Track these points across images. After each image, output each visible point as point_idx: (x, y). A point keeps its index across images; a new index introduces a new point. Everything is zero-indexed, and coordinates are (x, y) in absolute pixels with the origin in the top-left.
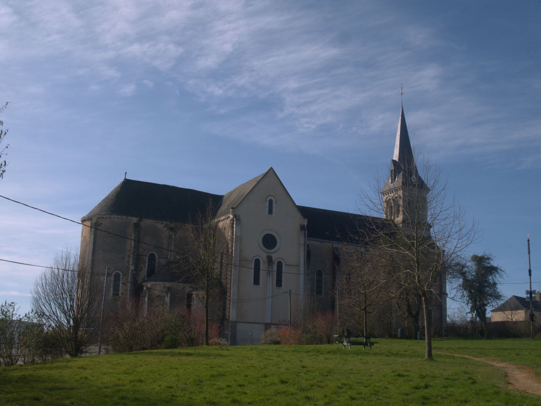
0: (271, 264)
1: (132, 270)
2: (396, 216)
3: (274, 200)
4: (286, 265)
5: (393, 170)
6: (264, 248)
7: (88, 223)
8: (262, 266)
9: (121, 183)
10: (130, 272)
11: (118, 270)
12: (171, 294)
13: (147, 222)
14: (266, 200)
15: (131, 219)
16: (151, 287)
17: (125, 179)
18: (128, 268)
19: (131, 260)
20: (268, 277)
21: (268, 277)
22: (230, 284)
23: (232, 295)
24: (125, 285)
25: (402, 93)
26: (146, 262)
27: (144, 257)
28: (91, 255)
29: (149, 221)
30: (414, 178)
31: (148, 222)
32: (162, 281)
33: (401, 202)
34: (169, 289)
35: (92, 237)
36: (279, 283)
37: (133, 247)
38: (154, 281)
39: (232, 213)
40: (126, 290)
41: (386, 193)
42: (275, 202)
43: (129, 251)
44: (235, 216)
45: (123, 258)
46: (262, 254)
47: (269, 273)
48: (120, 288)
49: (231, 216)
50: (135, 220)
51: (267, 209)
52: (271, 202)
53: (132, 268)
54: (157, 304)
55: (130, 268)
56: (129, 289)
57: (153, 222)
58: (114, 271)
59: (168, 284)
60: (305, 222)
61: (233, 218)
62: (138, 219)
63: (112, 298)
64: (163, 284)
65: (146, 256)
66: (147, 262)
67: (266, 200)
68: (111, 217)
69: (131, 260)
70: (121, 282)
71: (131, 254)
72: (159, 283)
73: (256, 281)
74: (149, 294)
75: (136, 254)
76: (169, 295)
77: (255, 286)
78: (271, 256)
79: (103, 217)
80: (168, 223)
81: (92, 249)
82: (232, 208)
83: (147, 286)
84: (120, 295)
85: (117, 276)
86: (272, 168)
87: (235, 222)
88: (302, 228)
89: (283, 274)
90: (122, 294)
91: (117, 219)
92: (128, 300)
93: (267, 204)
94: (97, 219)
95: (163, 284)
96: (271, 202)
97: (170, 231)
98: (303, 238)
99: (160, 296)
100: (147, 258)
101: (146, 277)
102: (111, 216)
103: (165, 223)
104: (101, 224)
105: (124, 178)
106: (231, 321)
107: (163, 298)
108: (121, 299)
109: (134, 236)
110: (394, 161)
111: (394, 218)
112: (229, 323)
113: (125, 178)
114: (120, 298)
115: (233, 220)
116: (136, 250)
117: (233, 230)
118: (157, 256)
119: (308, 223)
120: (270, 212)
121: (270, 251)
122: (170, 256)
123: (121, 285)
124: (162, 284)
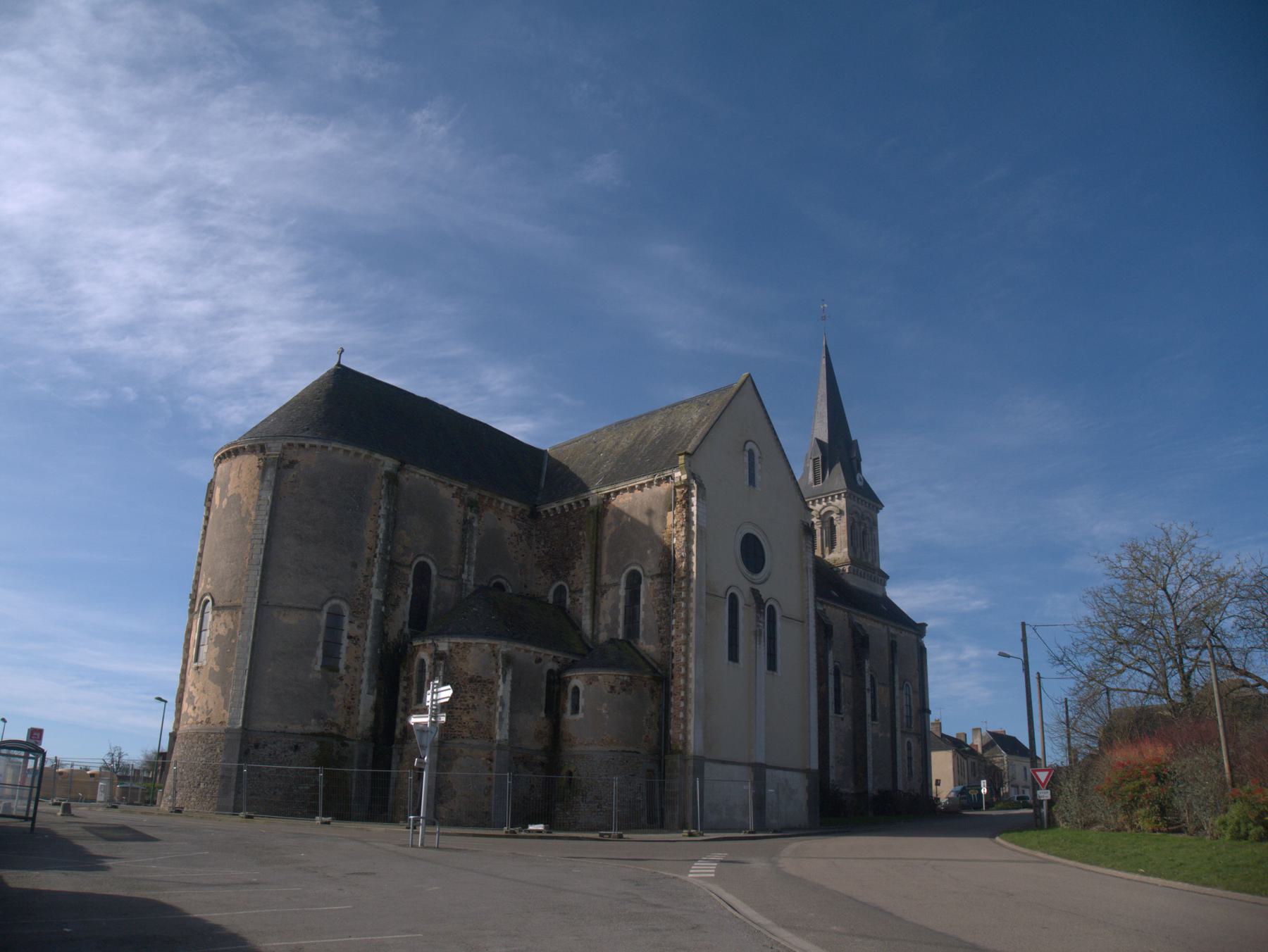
2: (827, 549)
5: (818, 458)
7: (250, 462)
9: (328, 372)
10: (372, 607)
11: (341, 598)
13: (417, 477)
14: (744, 450)
15: (379, 460)
16: (451, 651)
17: (339, 364)
18: (366, 596)
19: (376, 575)
22: (686, 655)
23: (692, 686)
24: (355, 644)
25: (825, 316)
26: (408, 586)
27: (404, 570)
28: (263, 547)
29: (422, 475)
31: (417, 476)
32: (488, 635)
33: (841, 526)
34: (508, 660)
35: (268, 496)
37: (381, 536)
38: (459, 633)
39: (685, 467)
41: (839, 495)
42: (760, 458)
43: (369, 548)
44: (692, 475)
45: (355, 565)
47: (757, 634)
48: (343, 649)
49: (680, 475)
50: (389, 464)
53: (376, 595)
54: (470, 702)
55: (371, 596)
56: (367, 654)
57: (430, 478)
58: (330, 599)
59: (503, 647)
61: (688, 480)
62: (397, 463)
63: (320, 677)
64: (490, 645)
65: (410, 566)
66: (411, 586)
67: (744, 450)
68: (327, 447)
69: (376, 575)
70: (345, 634)
71: (375, 556)
73: (733, 656)
74: (445, 673)
75: (388, 558)
76: (509, 677)
77: (731, 663)
78: (758, 591)
79: (303, 446)
80: (465, 487)
81: (265, 530)
82: (686, 454)
83: (436, 650)
84: (342, 671)
85: (335, 616)
87: (694, 492)
90: (347, 668)
91: (343, 453)
93: (746, 460)
94: (284, 448)
95: (490, 645)
96: (751, 453)
97: (469, 508)
99: (479, 679)
100: (412, 572)
101: (407, 626)
102: (326, 444)
103: (457, 484)
105: (336, 363)
106: (696, 758)
107: (490, 686)
108: (344, 683)
109: (386, 508)
110: (819, 442)
111: (823, 553)
112: (685, 761)
113: (339, 362)
114: (341, 679)
115: (687, 485)
116: (389, 548)
117: (689, 513)
118: (434, 572)
122: (469, 575)
123: (345, 641)
124: (486, 643)
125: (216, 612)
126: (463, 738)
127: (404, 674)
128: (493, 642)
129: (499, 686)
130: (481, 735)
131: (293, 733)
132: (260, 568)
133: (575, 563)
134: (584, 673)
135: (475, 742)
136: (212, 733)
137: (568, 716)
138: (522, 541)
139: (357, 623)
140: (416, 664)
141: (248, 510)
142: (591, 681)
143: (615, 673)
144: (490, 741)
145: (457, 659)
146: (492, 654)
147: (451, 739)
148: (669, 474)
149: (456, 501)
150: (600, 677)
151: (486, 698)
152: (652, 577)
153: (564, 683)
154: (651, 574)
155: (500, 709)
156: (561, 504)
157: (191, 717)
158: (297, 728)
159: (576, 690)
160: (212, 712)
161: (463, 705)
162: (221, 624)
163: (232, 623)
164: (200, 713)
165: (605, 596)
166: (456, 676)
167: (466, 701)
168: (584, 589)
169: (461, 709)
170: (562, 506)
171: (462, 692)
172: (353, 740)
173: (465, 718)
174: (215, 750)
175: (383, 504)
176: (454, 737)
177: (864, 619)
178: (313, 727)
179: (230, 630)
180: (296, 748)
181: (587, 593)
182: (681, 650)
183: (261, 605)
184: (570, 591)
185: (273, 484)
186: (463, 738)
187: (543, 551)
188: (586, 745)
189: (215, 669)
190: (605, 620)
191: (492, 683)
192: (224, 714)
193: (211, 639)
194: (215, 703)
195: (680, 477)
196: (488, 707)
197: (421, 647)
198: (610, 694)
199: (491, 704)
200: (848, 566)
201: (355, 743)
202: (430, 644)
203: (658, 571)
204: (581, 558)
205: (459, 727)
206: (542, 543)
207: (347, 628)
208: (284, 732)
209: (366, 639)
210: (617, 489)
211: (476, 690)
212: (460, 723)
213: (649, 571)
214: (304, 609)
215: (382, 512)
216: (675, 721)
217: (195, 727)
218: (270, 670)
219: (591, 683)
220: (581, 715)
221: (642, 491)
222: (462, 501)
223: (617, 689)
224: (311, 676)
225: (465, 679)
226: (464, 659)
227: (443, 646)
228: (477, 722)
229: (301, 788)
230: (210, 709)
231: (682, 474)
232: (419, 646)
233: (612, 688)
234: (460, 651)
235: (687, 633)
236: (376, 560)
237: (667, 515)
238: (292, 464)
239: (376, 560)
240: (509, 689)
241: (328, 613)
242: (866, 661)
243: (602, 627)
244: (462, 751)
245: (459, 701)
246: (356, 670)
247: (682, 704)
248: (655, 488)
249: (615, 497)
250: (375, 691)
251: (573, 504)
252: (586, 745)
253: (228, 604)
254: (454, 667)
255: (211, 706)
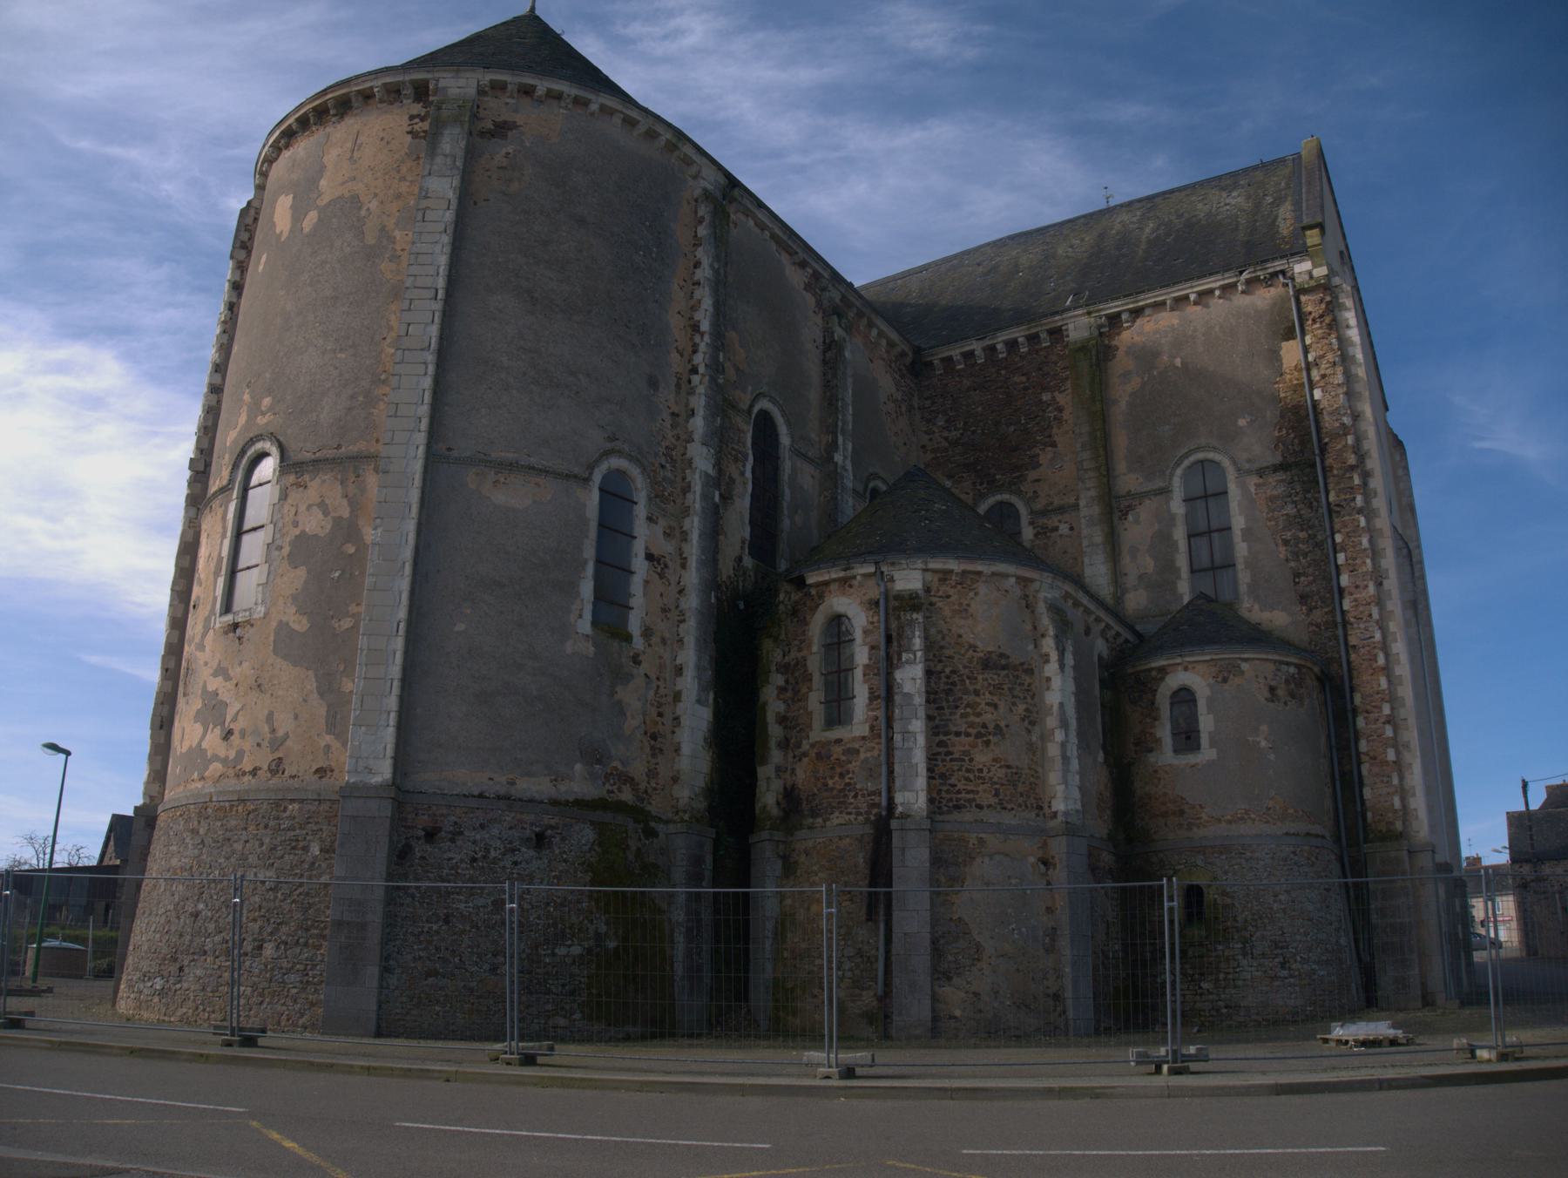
10: (698, 488)
11: (630, 458)
16: (928, 590)
28: (438, 306)
37: (705, 326)
48: (637, 584)
54: (989, 717)
55: (690, 462)
56: (692, 602)
58: (607, 454)
70: (639, 548)
71: (694, 371)
72: (1001, 567)
76: (1069, 660)
84: (638, 643)
85: (615, 496)
90: (647, 633)
92: (689, 684)
94: (481, 92)
95: (1019, 578)
99: (1003, 662)
109: (711, 266)
123: (639, 565)
125: (292, 478)
126: (979, 807)
127: (773, 654)
129: (1049, 679)
130: (1020, 800)
131: (531, 801)
132: (430, 358)
133: (1039, 455)
134: (1208, 658)
135: (1008, 819)
136: (293, 801)
137: (1166, 755)
138: (901, 414)
139: (662, 522)
140: (817, 625)
141: (383, 228)
142: (1224, 675)
143: (1276, 657)
144: (1038, 815)
145: (947, 613)
146: (1024, 603)
147: (949, 812)
148: (1278, 269)
149: (810, 300)
150: (1245, 666)
151: (1021, 707)
152: (1260, 472)
153: (1145, 686)
154: (1256, 466)
155: (1059, 736)
156: (988, 342)
157: (216, 758)
158: (537, 786)
159: (1184, 697)
160: (289, 743)
161: (971, 725)
162: (309, 507)
163: (345, 502)
164: (248, 745)
165: (1130, 518)
166: (947, 652)
167: (979, 715)
168: (1082, 503)
169: (968, 735)
170: (992, 348)
171: (966, 692)
172: (667, 822)
173: (982, 758)
174: (306, 849)
175: (704, 255)
176: (958, 807)
178: (580, 784)
179: (338, 521)
180: (540, 841)
181: (1089, 509)
182: (1370, 615)
183: (433, 460)
184: (1032, 512)
185: (459, 164)
186: (979, 807)
187: (946, 439)
188: (1229, 822)
189: (296, 627)
190: (1140, 564)
191: (1030, 672)
192: (328, 747)
193: (280, 548)
194: (296, 717)
195: (1310, 273)
196: (1029, 732)
197: (834, 587)
198: (1271, 705)
199: (1033, 723)
201: (672, 828)
202: (865, 576)
203: (1277, 459)
204: (1054, 445)
205: (968, 779)
206: (941, 423)
207: (644, 535)
208: (507, 798)
209: (684, 566)
210: (1141, 304)
211: (999, 687)
212: (968, 771)
213: (1249, 461)
214: (545, 472)
215: (704, 273)
216: (1376, 770)
217: (232, 784)
218: (461, 627)
219: (1225, 680)
220: (1207, 753)
221: (1207, 306)
222: (819, 304)
223: (1281, 692)
224: (569, 647)
225: (970, 661)
226: (963, 611)
227: (908, 579)
228: (1008, 767)
229: (561, 951)
230: (280, 733)
231: (1315, 266)
232: (826, 583)
233: (1272, 689)
234: (951, 591)
235: (1379, 578)
236: (696, 379)
237: (1281, 348)
238: (502, 129)
239: (696, 379)
240: (1071, 687)
241: (601, 490)
243: (1131, 580)
244: (981, 841)
245: (963, 716)
246: (664, 641)
247: (1389, 732)
248: (1244, 301)
249: (1134, 321)
250: (711, 697)
251: (1020, 340)
252: (1229, 822)
253: (330, 453)
254: (940, 632)
255: (285, 724)
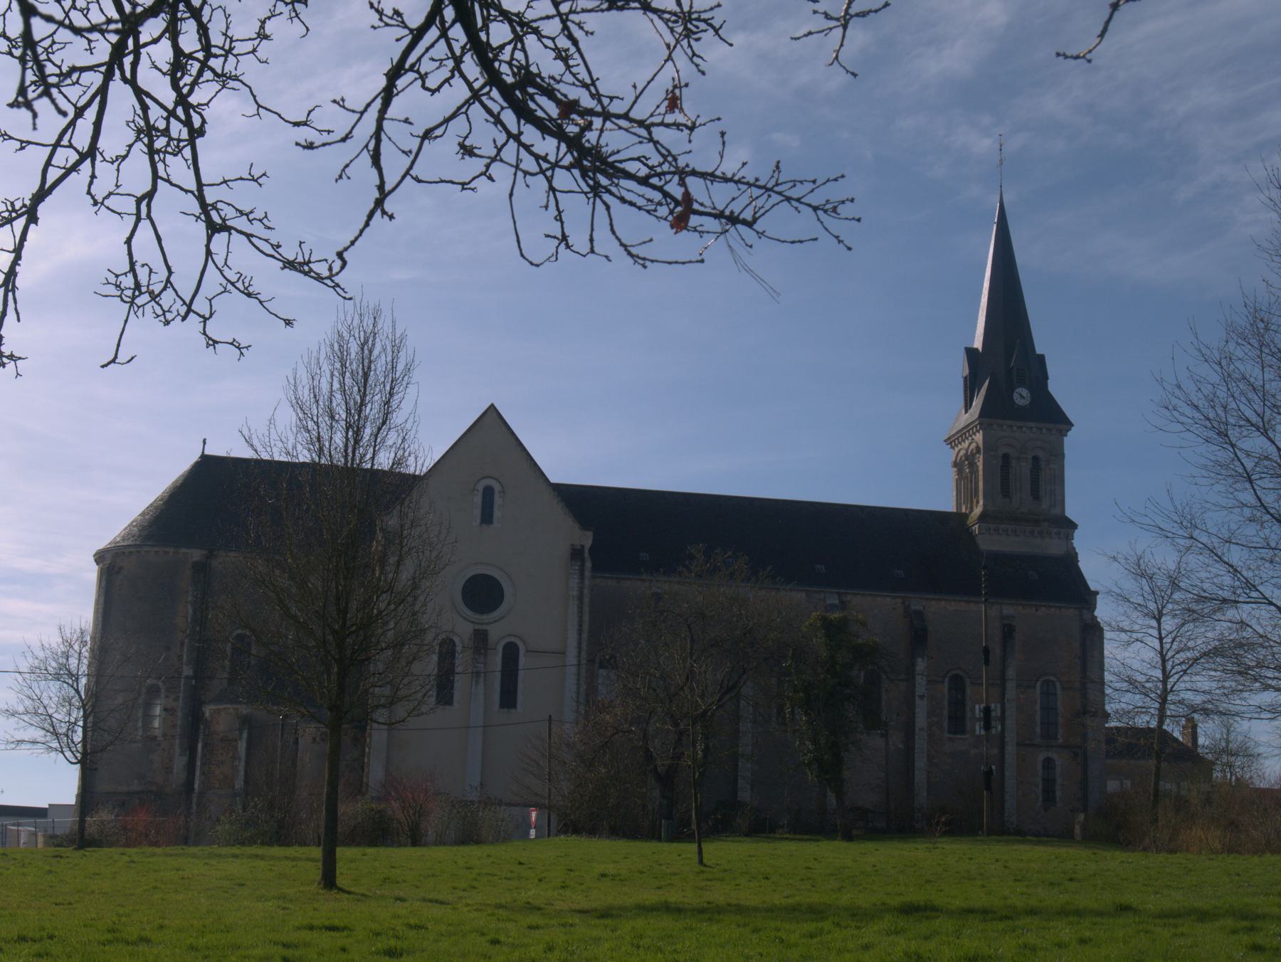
0: (483, 651)
1: (187, 678)
3: (497, 487)
4: (527, 651)
6: (469, 613)
8: (462, 661)
12: (248, 734)
20: (474, 683)
21: (474, 683)
30: (1022, 396)
34: (246, 721)
36: (508, 698)
37: (189, 620)
40: (174, 726)
42: (499, 492)
46: (461, 625)
50: (196, 555)
51: (477, 512)
52: (488, 492)
53: (187, 671)
56: (179, 722)
59: (244, 710)
60: (587, 539)
64: (234, 709)
72: (226, 706)
76: (245, 735)
86: (492, 405)
88: (576, 554)
89: (521, 674)
92: (177, 750)
93: (478, 499)
95: (234, 709)
96: (488, 492)
98: (577, 581)
104: (121, 568)
105: (200, 454)
110: (971, 352)
116: (198, 629)
119: (594, 540)
120: (487, 517)
121: (485, 617)
128: (236, 706)
151: (231, 754)
177: (943, 603)
200: (977, 526)
223: (318, 739)
233: (314, 739)
242: (920, 660)
250: (188, 753)
